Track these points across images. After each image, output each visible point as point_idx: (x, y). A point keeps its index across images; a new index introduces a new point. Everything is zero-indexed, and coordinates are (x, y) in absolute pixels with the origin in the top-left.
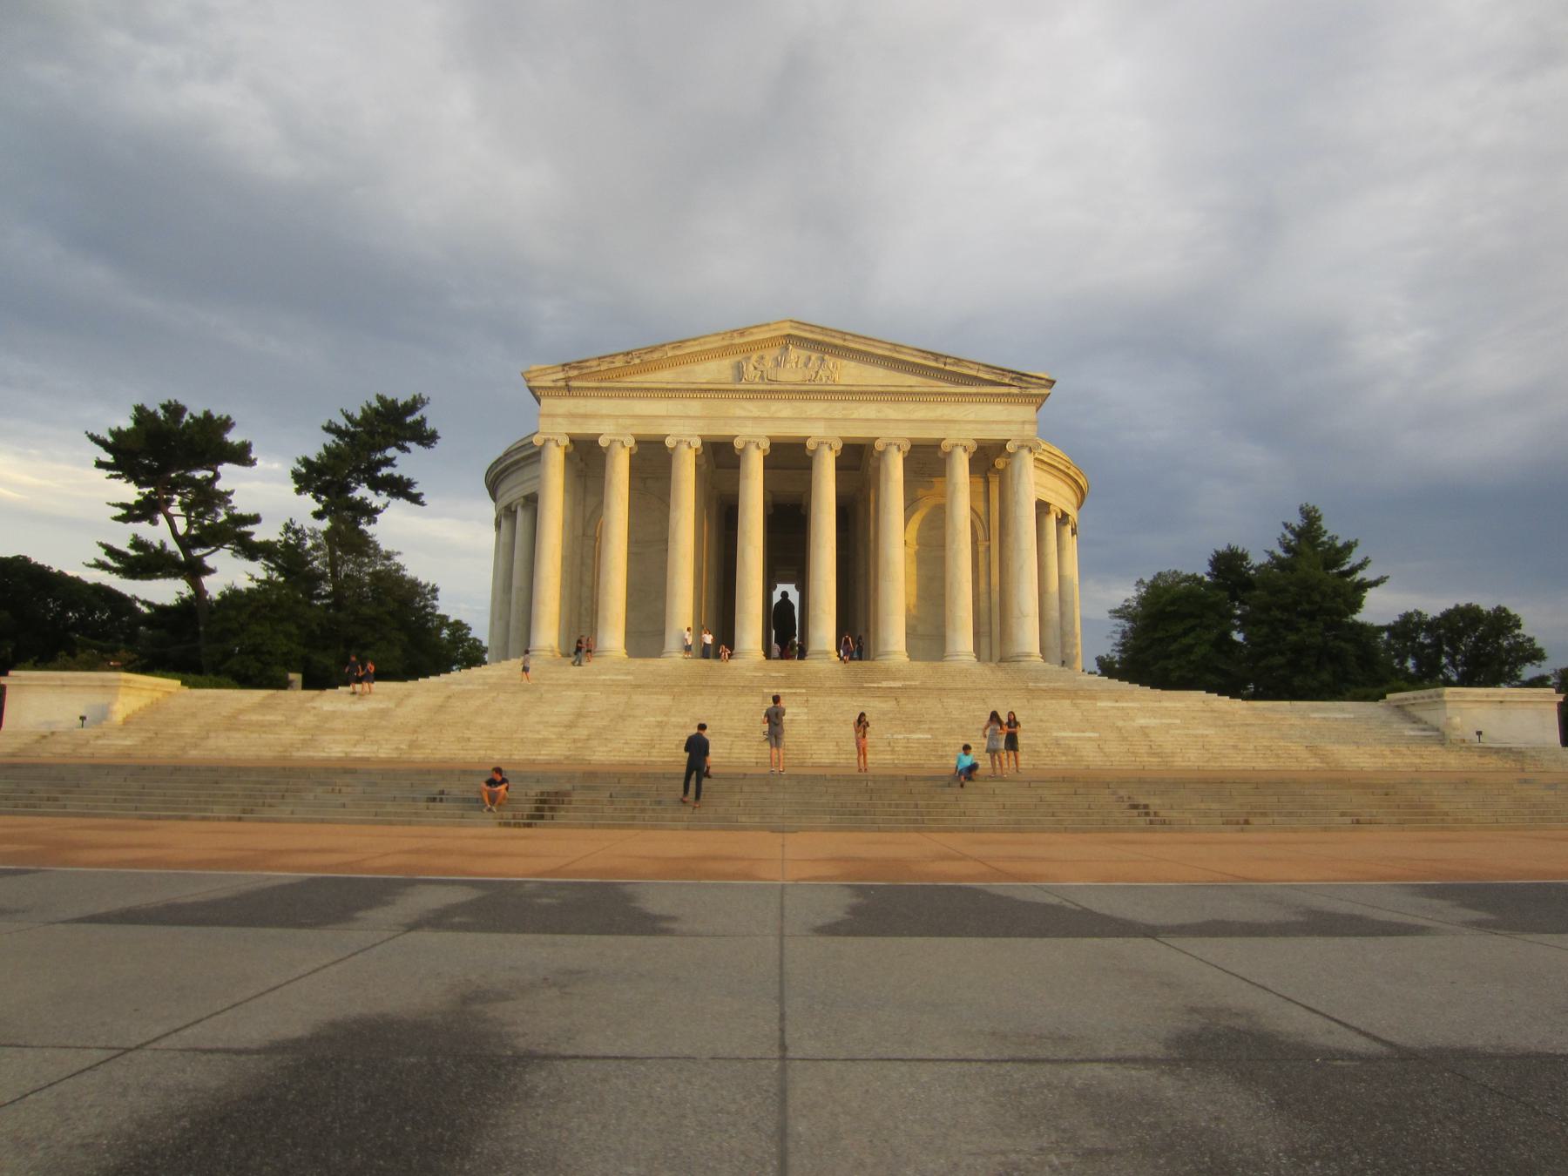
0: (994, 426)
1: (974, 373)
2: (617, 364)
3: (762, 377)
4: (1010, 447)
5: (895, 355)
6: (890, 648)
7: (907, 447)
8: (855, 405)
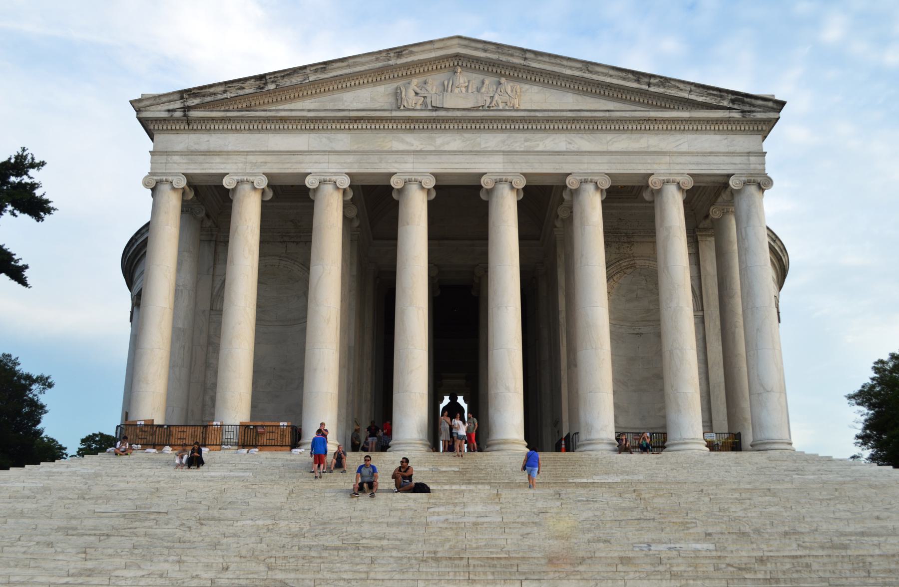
0: (712, 159)
1: (685, 95)
2: (247, 91)
3: (425, 104)
4: (733, 183)
5: (587, 75)
6: (594, 436)
8: (539, 136)
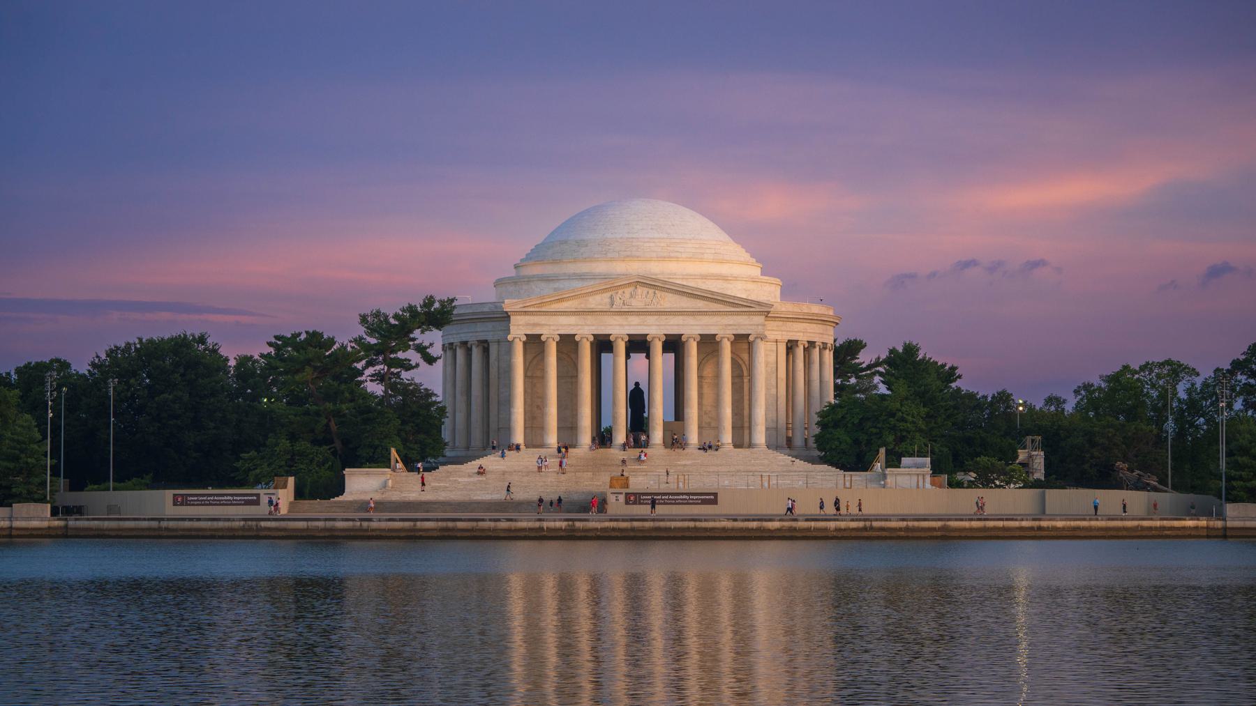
7: (698, 339)
